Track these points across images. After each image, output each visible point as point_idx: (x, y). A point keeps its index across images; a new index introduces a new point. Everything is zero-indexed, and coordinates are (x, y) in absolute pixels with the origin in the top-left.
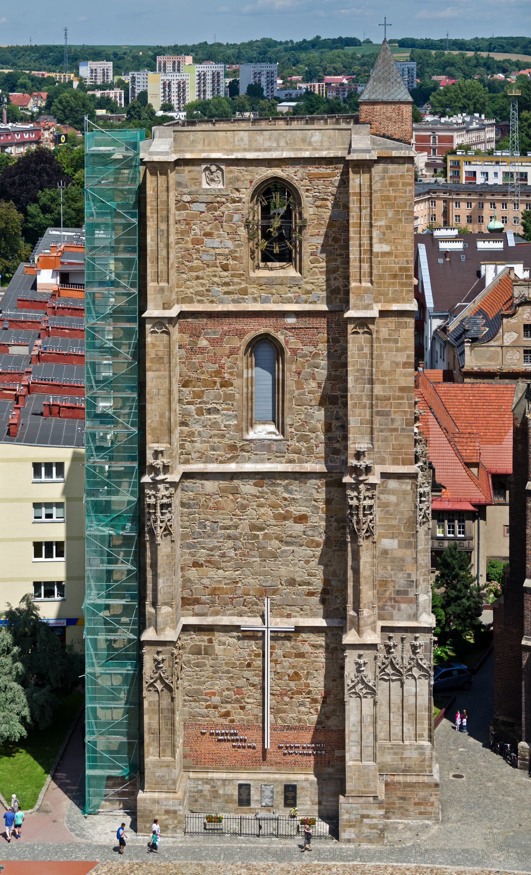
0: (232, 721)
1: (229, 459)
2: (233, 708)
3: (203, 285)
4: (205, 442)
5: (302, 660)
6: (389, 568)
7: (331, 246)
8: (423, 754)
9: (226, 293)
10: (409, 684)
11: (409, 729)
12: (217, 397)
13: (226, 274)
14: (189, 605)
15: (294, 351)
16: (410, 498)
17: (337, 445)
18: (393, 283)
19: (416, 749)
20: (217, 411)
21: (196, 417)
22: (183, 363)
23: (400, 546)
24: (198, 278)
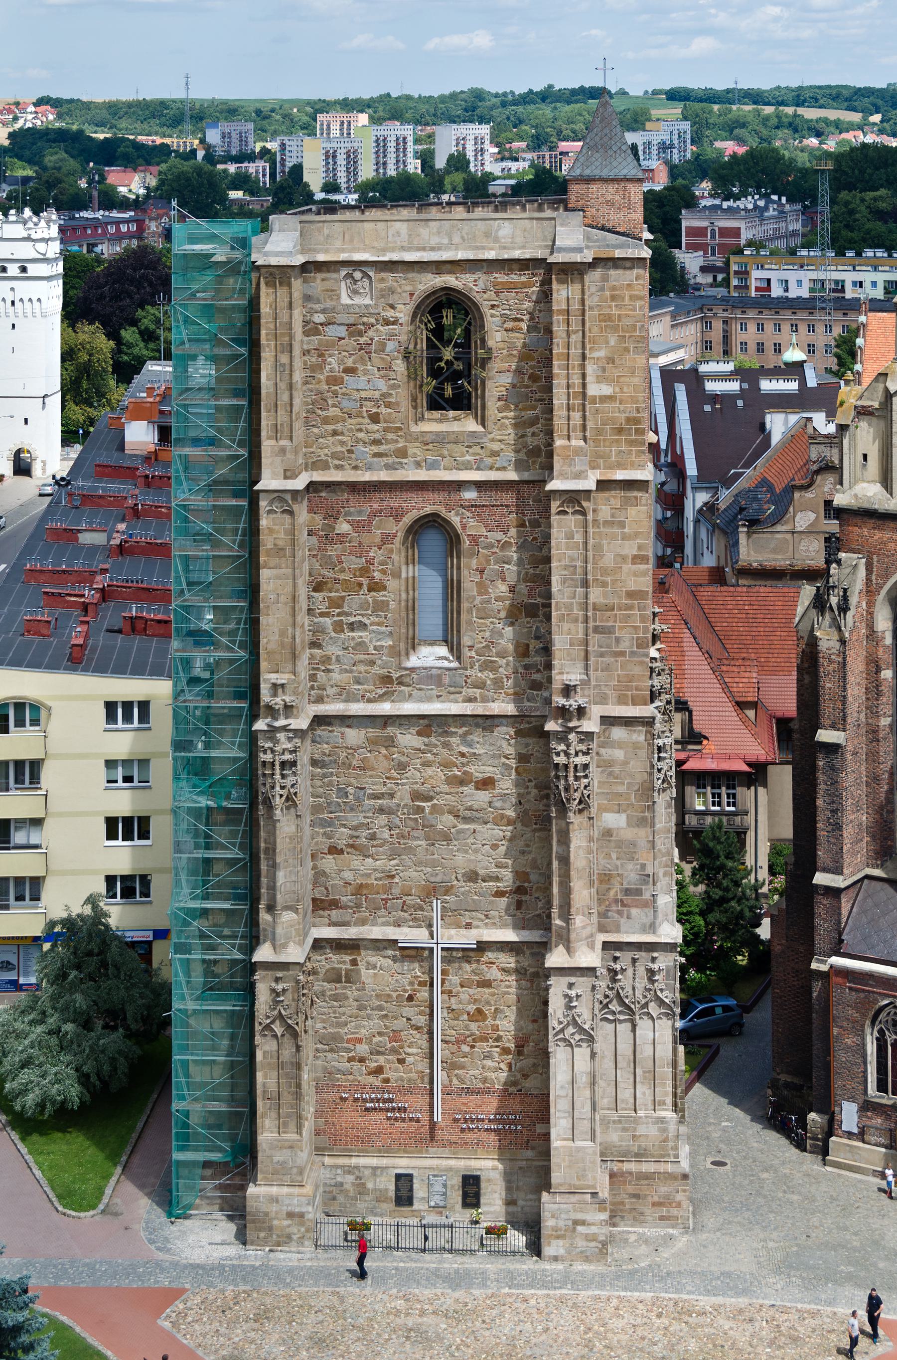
0: (387, 1081)
1: (381, 696)
2: (388, 1061)
3: (343, 443)
4: (346, 671)
5: (487, 990)
6: (614, 856)
7: (527, 387)
8: (665, 1130)
10: (644, 1026)
11: (644, 1094)
12: (364, 606)
13: (375, 427)
14: (323, 909)
15: (474, 539)
16: (643, 753)
17: (537, 677)
18: (617, 441)
20: (363, 626)
21: (333, 634)
22: (314, 556)
23: (629, 824)
24: (335, 433)
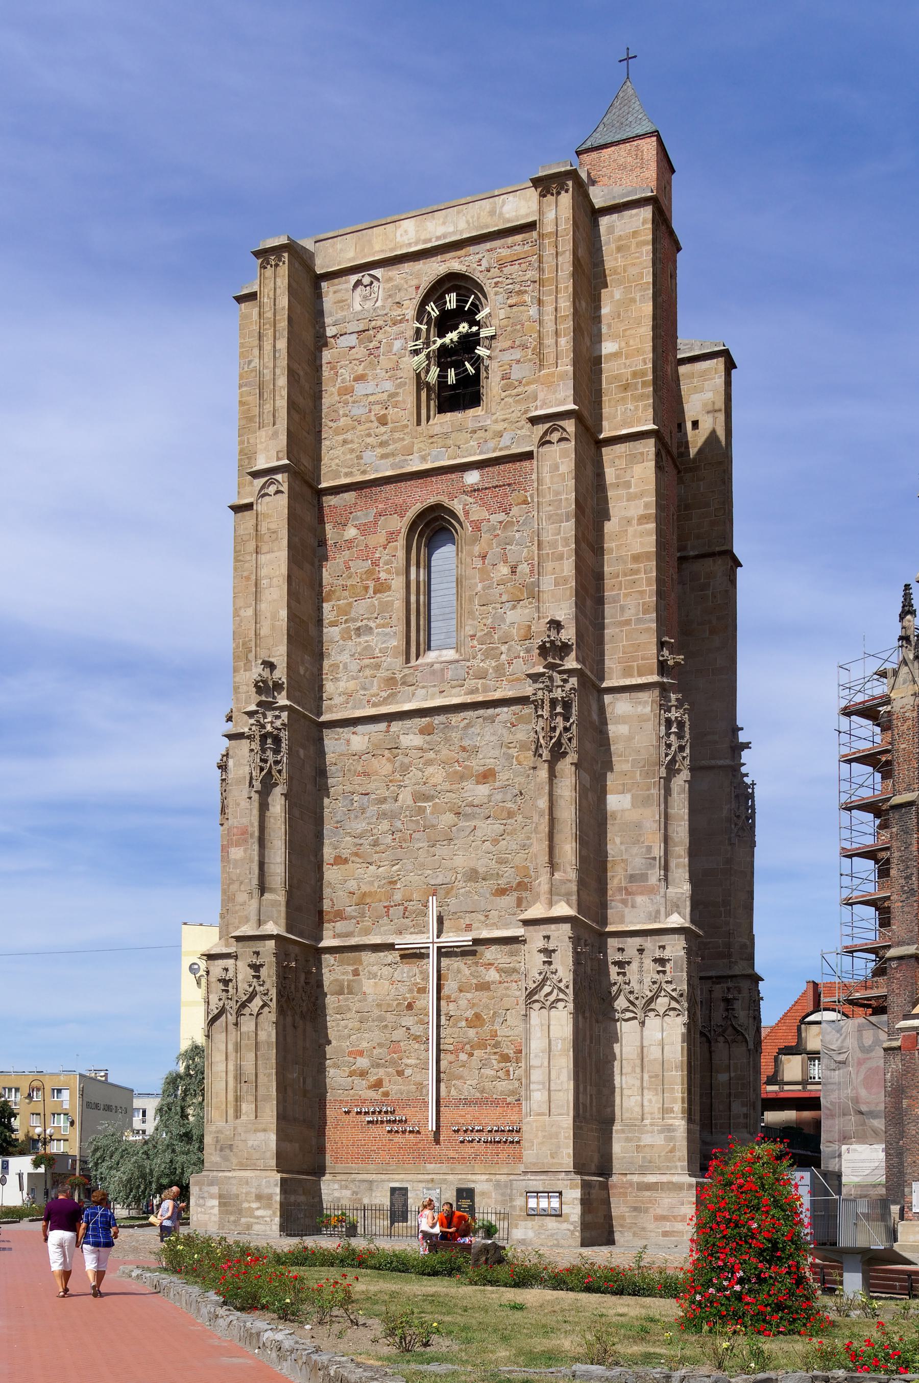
0: (386, 1094)
1: (385, 699)
2: (388, 1074)
3: (352, 451)
4: (354, 678)
5: (486, 994)
9: (384, 456)
11: (650, 1101)
13: (383, 429)
18: (623, 398)
19: (661, 1132)
21: (341, 642)
24: (345, 442)
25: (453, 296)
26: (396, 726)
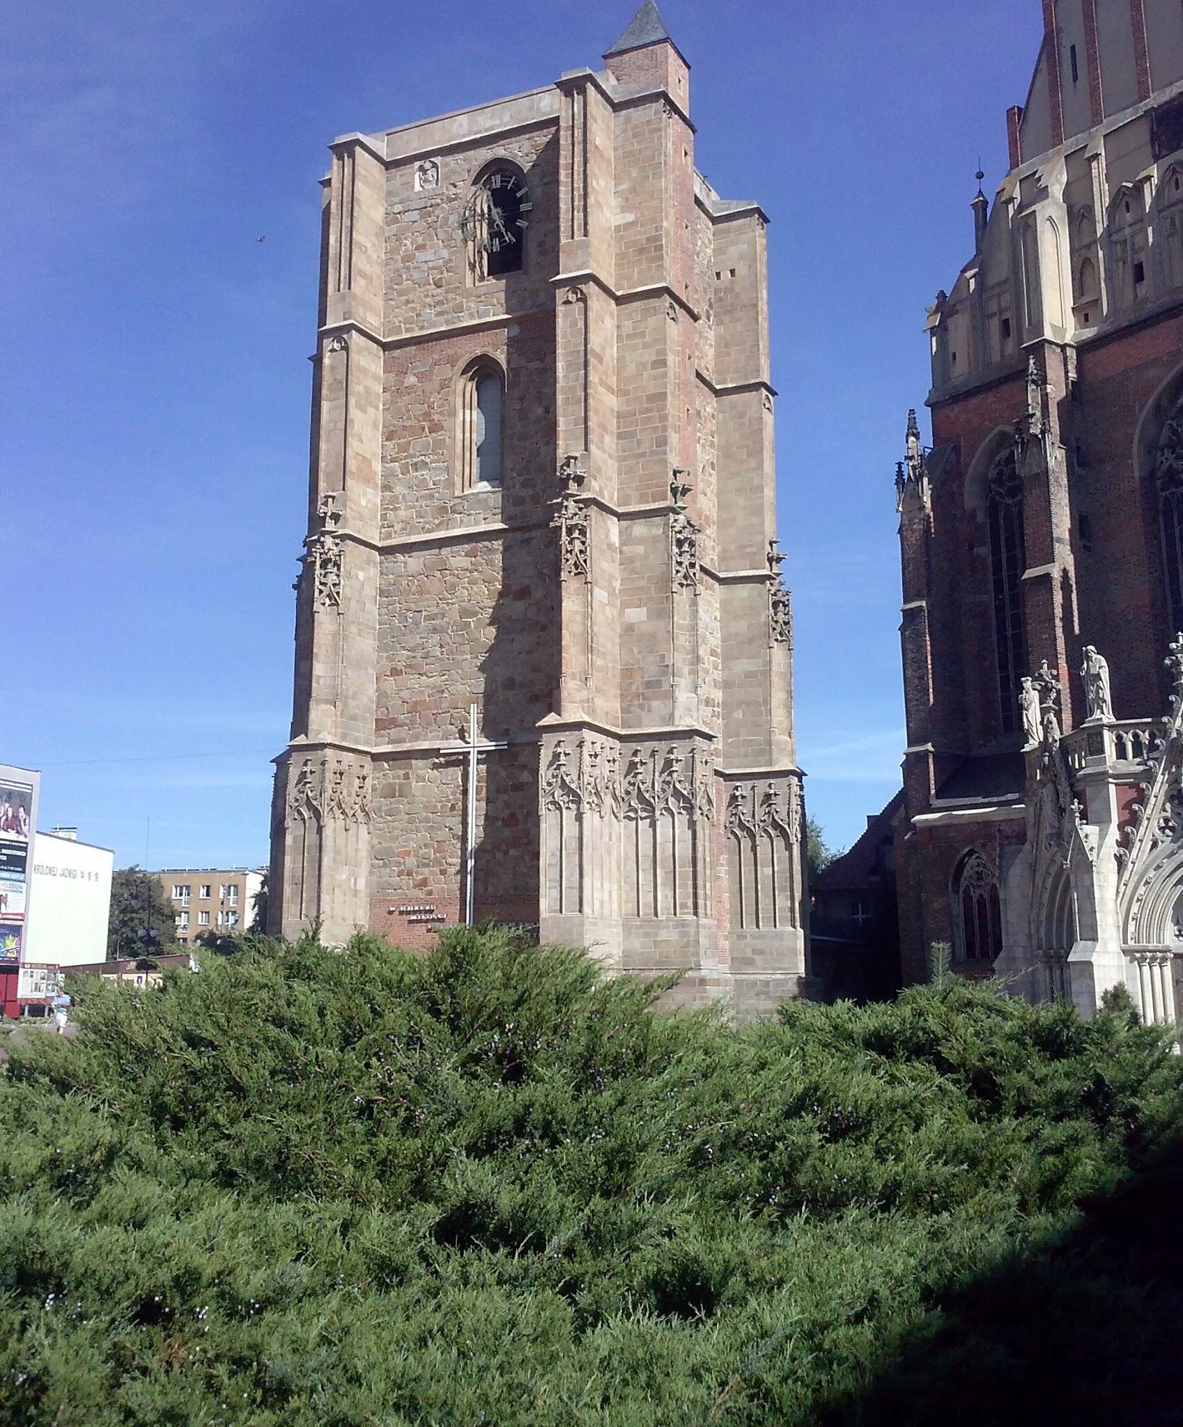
3: (413, 309)
6: (635, 650)
9: (441, 313)
13: (439, 290)
16: (661, 546)
24: (408, 302)
25: (499, 177)
26: (445, 551)
